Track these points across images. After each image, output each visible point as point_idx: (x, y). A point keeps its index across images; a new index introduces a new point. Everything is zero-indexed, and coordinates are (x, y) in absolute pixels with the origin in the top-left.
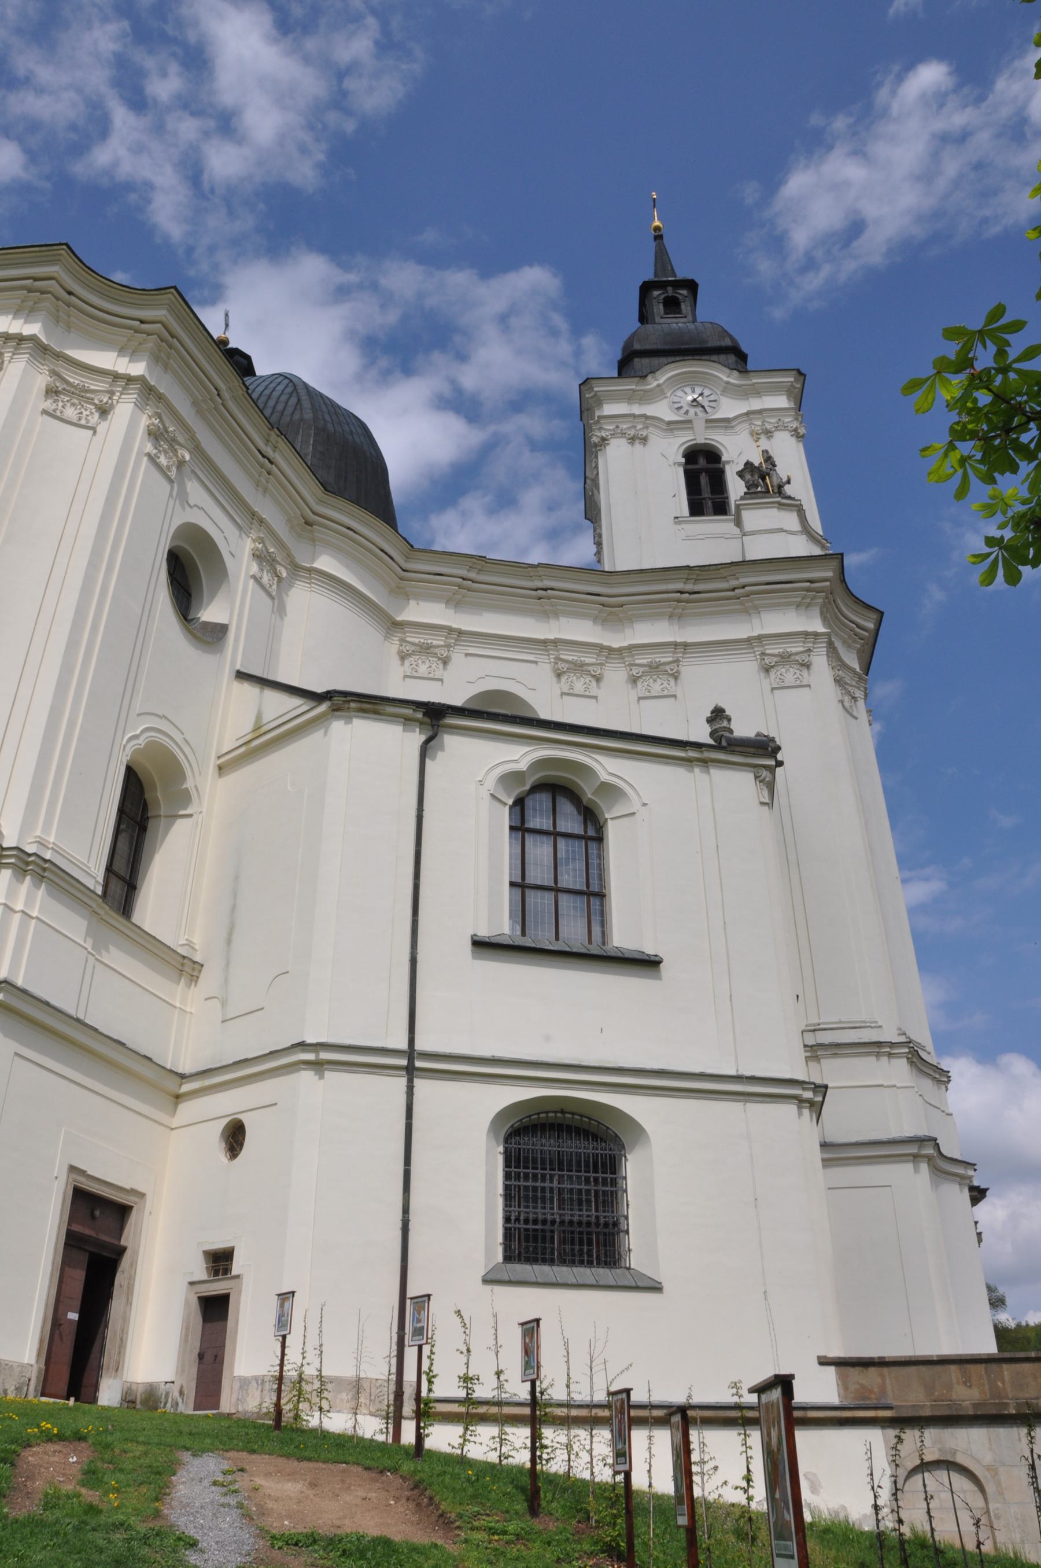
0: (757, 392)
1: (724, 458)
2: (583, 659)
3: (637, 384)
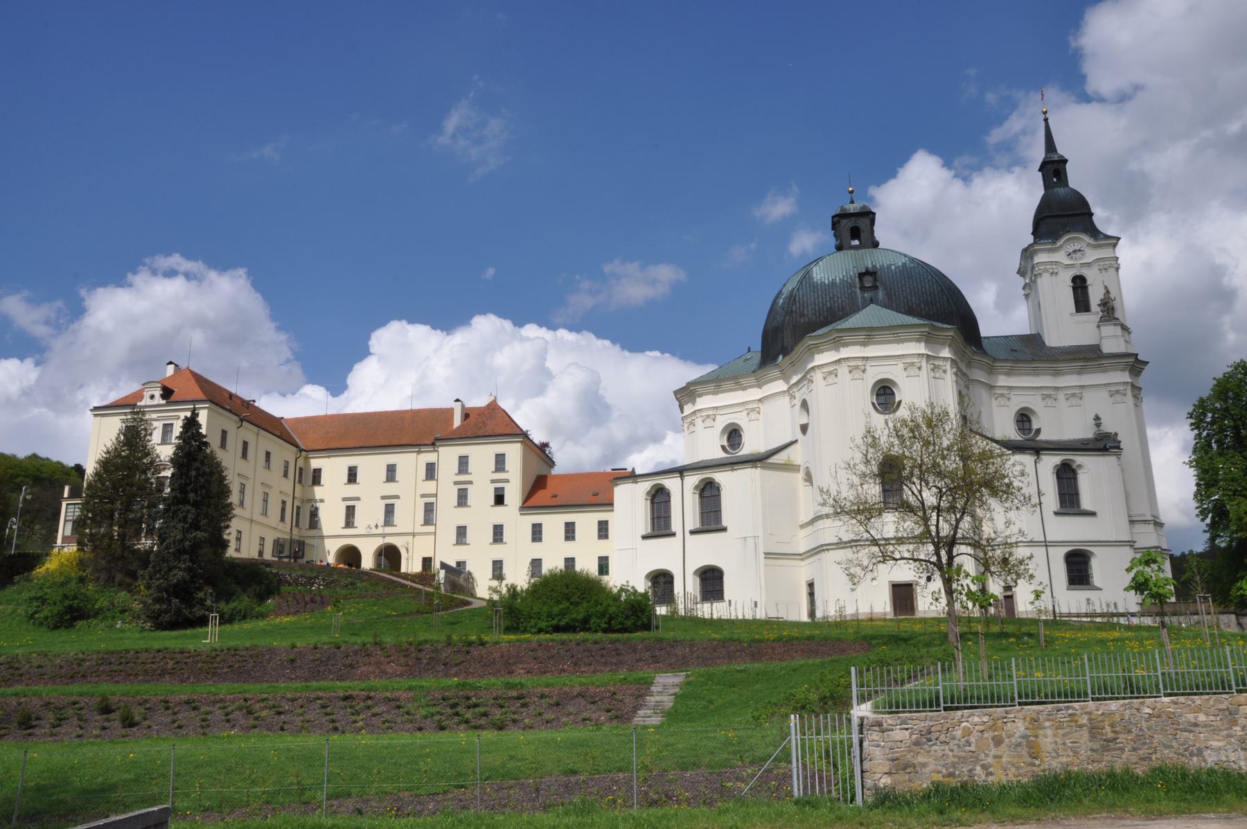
0: (1100, 246)
1: (1088, 283)
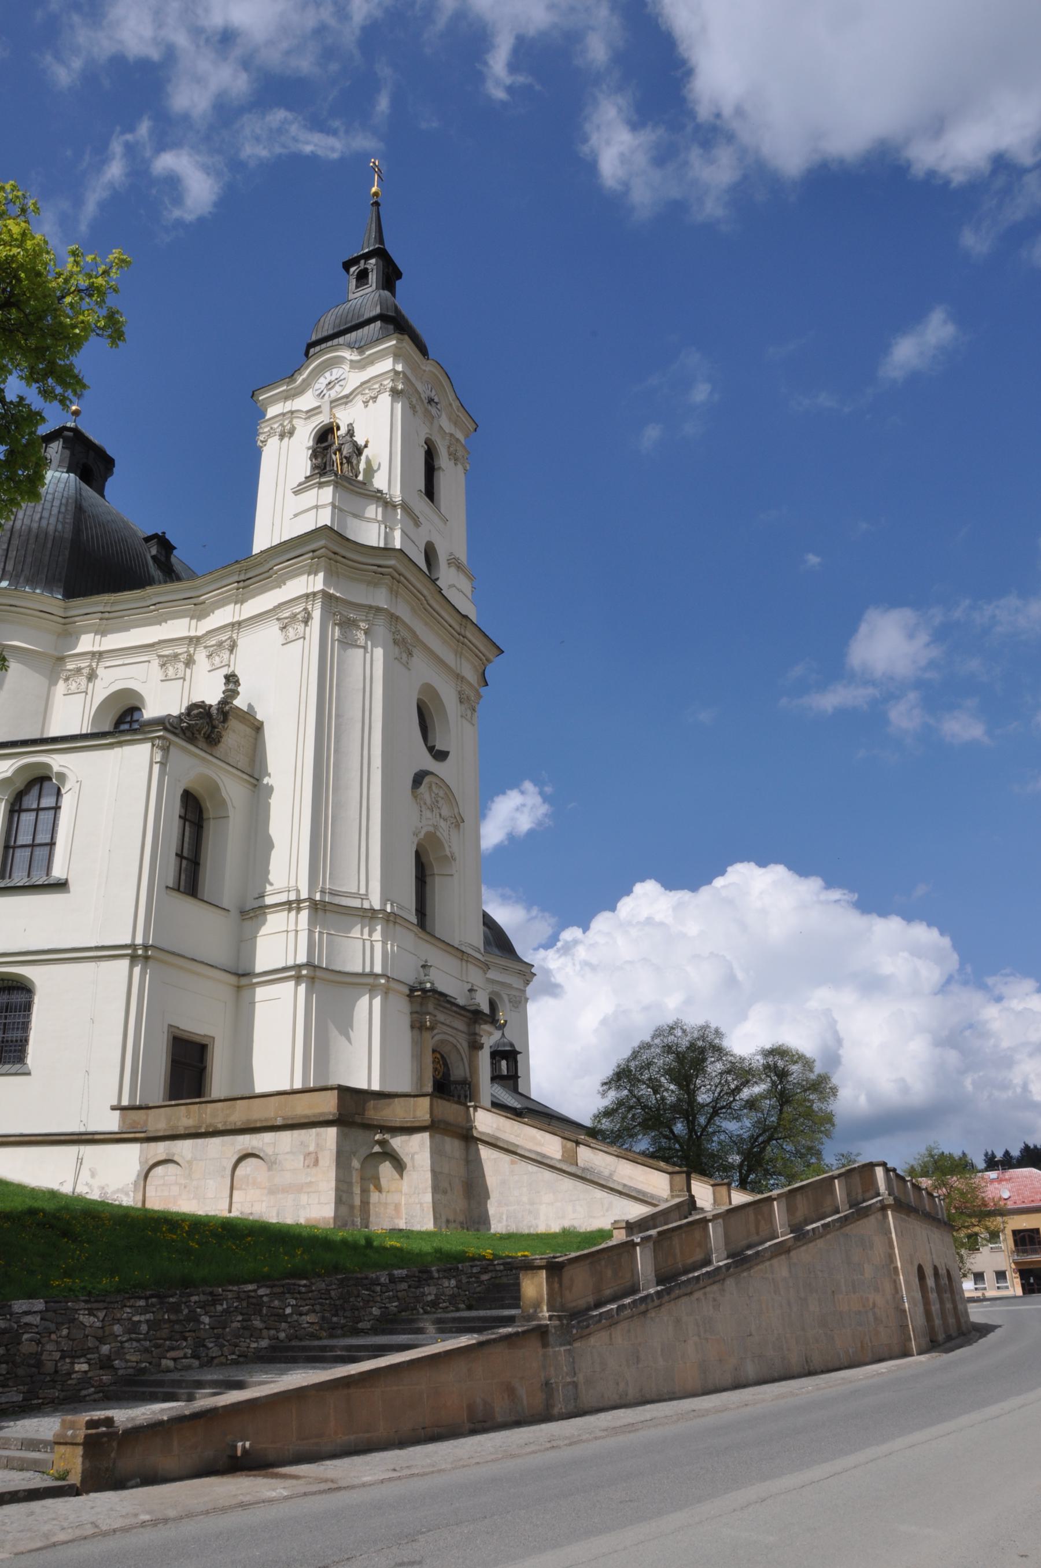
0: (371, 361)
2: (176, 651)
3: (288, 384)
